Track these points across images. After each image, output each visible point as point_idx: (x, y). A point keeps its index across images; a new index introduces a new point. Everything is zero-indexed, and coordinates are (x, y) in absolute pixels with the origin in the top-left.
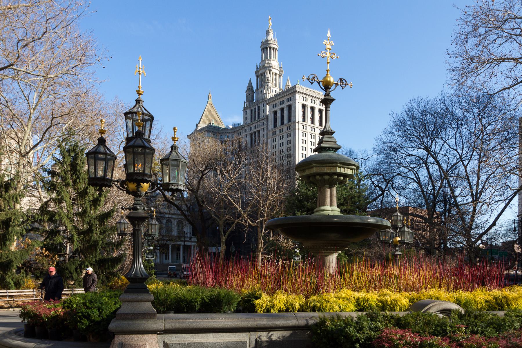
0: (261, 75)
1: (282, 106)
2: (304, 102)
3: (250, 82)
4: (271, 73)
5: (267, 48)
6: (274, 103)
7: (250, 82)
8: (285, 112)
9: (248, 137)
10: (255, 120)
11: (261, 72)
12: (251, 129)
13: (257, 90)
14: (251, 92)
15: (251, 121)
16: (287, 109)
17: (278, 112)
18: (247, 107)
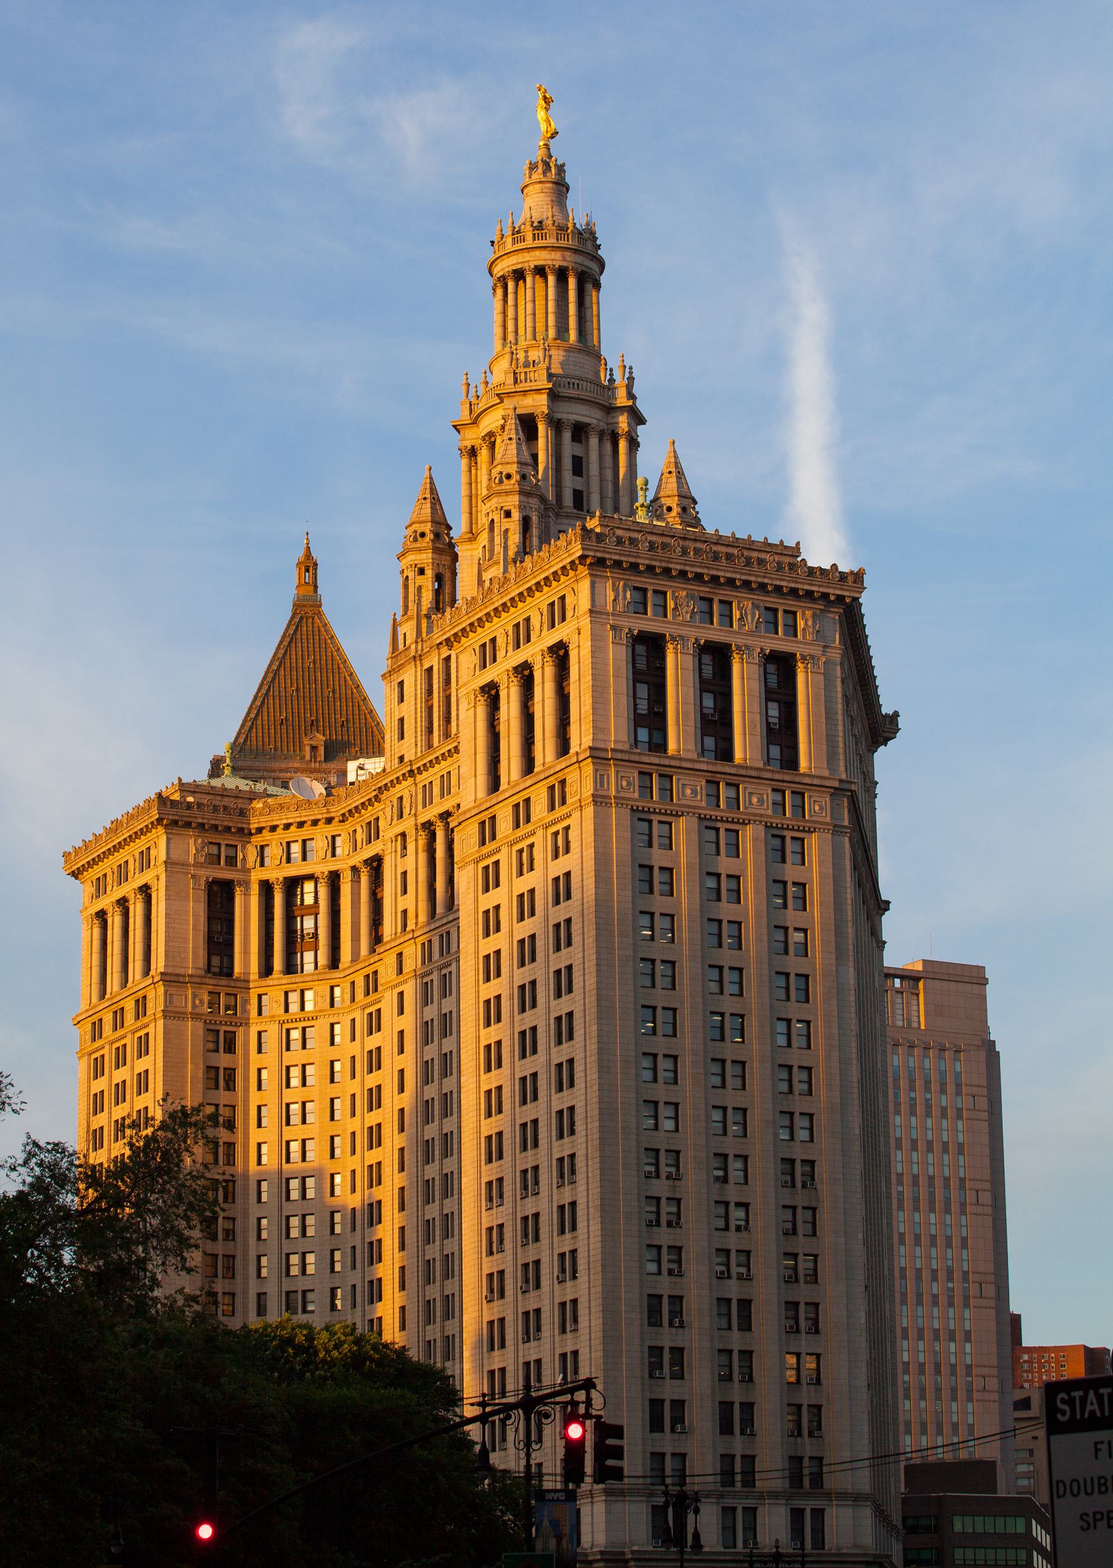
9: (411, 847)
15: (430, 746)
16: (550, 671)
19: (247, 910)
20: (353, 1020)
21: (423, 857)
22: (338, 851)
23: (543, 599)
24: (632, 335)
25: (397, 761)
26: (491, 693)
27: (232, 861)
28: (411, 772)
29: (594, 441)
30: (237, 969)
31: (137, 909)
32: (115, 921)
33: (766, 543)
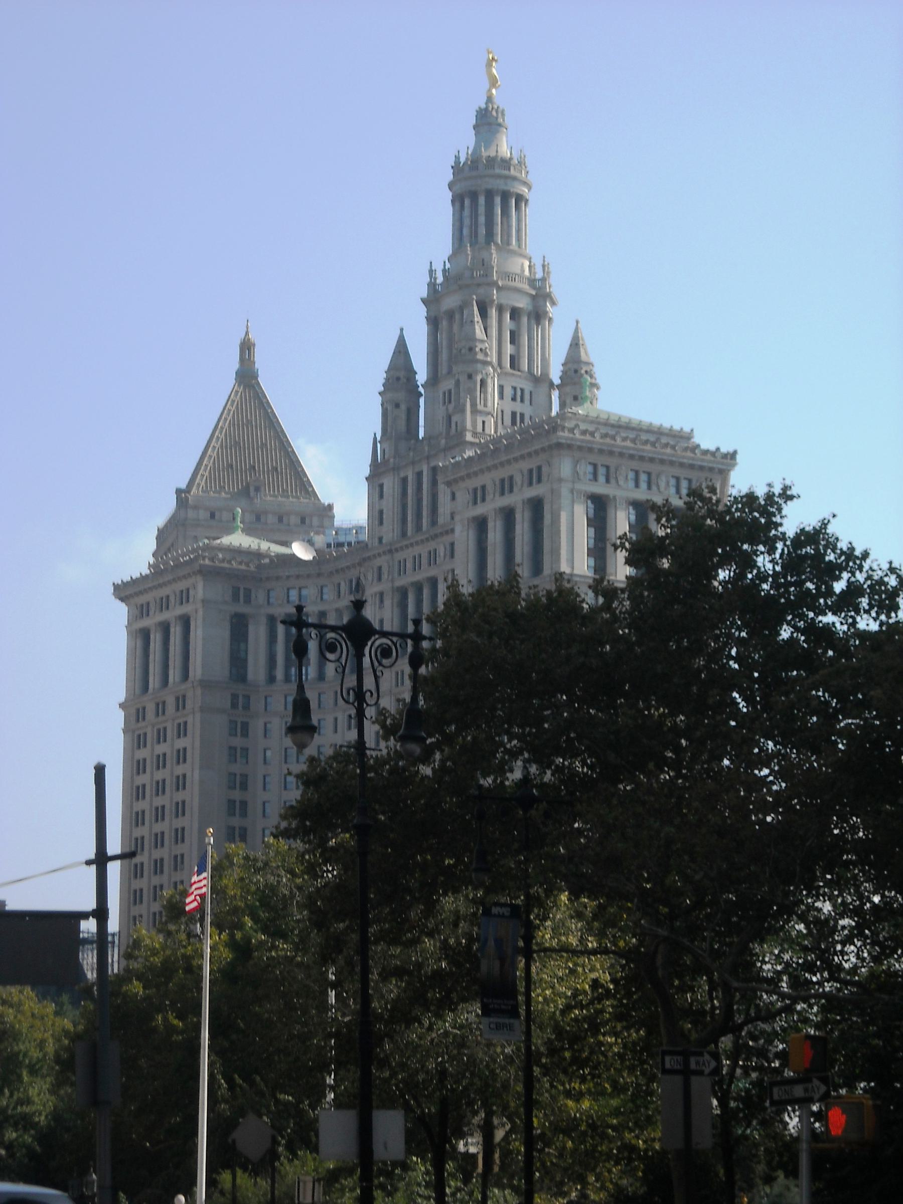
0: (450, 315)
1: (507, 501)
2: (600, 488)
3: (401, 350)
4: (493, 313)
5: (474, 196)
6: (477, 482)
7: (401, 350)
8: (518, 527)
9: (388, 602)
10: (418, 528)
11: (451, 302)
12: (402, 568)
13: (434, 379)
14: (401, 396)
15: (404, 534)
16: (527, 515)
17: (490, 525)
18: (385, 461)
19: (257, 633)
20: (336, 719)
21: (396, 611)
22: (325, 597)
23: (525, 465)
24: (546, 237)
25: (377, 540)
26: (481, 524)
27: (248, 600)
28: (390, 551)
29: (525, 320)
30: (250, 676)
31: (176, 632)
32: (156, 639)
33: (671, 429)
